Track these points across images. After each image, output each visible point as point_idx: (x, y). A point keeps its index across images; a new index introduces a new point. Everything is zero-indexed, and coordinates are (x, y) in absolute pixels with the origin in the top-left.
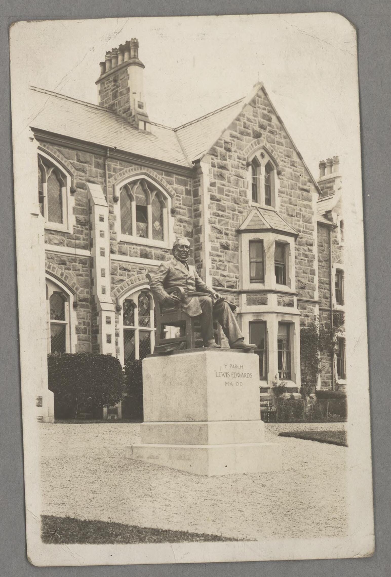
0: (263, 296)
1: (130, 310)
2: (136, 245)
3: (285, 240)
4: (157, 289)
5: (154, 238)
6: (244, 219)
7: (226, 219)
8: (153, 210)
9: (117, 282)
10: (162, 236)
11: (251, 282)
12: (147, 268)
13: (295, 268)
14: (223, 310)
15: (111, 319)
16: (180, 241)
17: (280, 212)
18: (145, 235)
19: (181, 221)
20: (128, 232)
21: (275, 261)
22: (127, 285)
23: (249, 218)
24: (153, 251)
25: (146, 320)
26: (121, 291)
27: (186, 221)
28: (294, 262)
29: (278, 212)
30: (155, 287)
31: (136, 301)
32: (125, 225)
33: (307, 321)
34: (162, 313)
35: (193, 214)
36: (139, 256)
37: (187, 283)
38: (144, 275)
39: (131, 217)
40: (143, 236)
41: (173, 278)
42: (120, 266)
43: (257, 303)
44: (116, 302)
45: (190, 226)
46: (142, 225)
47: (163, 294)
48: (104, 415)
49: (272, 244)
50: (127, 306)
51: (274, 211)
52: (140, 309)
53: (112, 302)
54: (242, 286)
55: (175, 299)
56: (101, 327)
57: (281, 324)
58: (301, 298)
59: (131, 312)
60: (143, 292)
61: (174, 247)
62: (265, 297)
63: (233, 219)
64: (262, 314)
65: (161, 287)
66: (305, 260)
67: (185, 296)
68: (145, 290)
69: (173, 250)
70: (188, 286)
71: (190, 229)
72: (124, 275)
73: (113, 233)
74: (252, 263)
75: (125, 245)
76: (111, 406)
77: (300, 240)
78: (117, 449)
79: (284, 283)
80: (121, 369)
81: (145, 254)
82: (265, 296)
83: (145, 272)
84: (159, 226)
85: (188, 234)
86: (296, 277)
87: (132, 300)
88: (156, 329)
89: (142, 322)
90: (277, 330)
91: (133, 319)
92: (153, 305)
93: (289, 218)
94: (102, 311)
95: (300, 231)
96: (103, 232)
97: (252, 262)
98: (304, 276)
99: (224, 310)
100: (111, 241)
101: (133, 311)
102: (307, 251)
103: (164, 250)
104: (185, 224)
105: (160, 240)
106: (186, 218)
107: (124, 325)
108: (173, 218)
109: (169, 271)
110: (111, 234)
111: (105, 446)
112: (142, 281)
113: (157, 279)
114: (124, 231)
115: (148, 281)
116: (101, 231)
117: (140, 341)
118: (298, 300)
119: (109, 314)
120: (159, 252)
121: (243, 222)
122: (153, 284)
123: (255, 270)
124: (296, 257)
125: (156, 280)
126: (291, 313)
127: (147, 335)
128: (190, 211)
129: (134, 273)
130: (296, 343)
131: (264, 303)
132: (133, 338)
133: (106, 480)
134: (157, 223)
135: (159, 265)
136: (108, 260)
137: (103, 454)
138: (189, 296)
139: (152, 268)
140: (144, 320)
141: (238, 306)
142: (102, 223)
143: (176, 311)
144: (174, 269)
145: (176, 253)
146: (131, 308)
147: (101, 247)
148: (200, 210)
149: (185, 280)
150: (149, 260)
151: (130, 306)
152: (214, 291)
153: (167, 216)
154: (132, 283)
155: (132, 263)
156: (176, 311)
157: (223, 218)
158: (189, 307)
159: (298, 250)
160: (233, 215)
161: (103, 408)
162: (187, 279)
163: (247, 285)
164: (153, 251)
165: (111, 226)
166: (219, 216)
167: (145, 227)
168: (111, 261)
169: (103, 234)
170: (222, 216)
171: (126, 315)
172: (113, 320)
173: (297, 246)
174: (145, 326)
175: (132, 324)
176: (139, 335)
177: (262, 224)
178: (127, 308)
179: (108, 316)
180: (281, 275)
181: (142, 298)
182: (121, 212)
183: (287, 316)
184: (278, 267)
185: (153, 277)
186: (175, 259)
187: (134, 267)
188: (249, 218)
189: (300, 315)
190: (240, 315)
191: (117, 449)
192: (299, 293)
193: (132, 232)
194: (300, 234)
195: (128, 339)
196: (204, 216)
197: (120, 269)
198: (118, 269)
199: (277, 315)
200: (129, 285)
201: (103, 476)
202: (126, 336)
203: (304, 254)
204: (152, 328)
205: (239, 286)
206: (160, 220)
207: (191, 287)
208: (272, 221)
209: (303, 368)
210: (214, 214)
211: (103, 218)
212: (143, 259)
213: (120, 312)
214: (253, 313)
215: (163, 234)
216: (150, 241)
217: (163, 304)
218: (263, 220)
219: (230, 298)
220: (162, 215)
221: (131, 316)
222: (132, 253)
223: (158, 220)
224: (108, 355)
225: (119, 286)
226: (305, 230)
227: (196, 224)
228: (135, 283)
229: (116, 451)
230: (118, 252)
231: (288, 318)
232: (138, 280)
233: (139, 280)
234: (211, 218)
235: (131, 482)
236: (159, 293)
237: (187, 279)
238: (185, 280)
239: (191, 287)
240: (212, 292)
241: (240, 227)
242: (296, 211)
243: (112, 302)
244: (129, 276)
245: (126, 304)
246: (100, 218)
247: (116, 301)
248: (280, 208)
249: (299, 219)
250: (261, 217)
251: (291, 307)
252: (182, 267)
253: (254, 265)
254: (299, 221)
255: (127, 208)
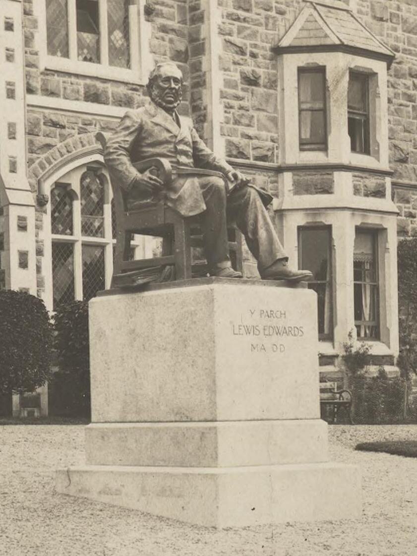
0: (325, 177)
1: (65, 204)
2: (77, 76)
3: (369, 66)
4: (118, 162)
5: (111, 63)
6: (288, 26)
7: (253, 27)
8: (109, 7)
9: (39, 149)
10: (126, 58)
11: (301, 150)
12: (99, 121)
13: (387, 122)
14: (247, 203)
15: (28, 222)
16: (162, 69)
17: (358, 12)
18: (94, 56)
19: (164, 29)
20: (61, 52)
21: (349, 107)
22: (58, 154)
23: (299, 25)
24: (110, 89)
25: (97, 224)
26: (48, 167)
27: (173, 30)
28: (386, 110)
29: (355, 12)
30: (114, 160)
31: (76, 186)
32: (54, 37)
33: (411, 226)
34: (126, 210)
35: (188, 16)
36: (82, 98)
37: (177, 152)
38: (92, 136)
39: (67, 21)
40: (90, 60)
41: (148, 141)
42: (45, 117)
43: (313, 190)
44: (36, 188)
45: (183, 40)
46: (88, 37)
47: (129, 172)
48: (14, 409)
49: (343, 75)
50: (59, 195)
51: (347, 11)
52: (84, 202)
53: (29, 188)
54: (284, 157)
55: (152, 182)
56: (9, 236)
57: (360, 231)
58: (400, 181)
59: (67, 207)
60: (89, 169)
61: (150, 80)
62: (329, 179)
63: (267, 25)
64: (323, 211)
65: (125, 159)
66: (408, 106)
67: (173, 177)
68: (94, 166)
69: (150, 86)
70: (178, 157)
71: (181, 46)
72: (52, 135)
73: (31, 54)
74: (303, 113)
75: (56, 77)
76: (28, 391)
77: (398, 66)
78: (39, 476)
79: (366, 151)
80: (48, 319)
81: (95, 94)
82: (329, 177)
83: (94, 130)
84: (121, 38)
85: (178, 56)
86: (390, 138)
87: (69, 185)
88: (115, 241)
89: (89, 228)
90: (353, 244)
91: (71, 220)
92: (110, 194)
93: (376, 25)
94: (10, 206)
95: (397, 50)
96: (13, 51)
97: (303, 110)
98: (405, 137)
99: (248, 204)
100: (28, 69)
101: (71, 205)
102: (411, 88)
103: (130, 86)
104: (171, 36)
105: (123, 66)
106: (174, 24)
107: (53, 232)
108: (149, 24)
109: (141, 128)
110: (28, 55)
111: (16, 470)
112: (88, 146)
113: (117, 142)
114: (52, 49)
115: (100, 147)
116: (7, 50)
117: (85, 264)
118: (393, 184)
119: (23, 212)
120: (122, 90)
121: (286, 32)
122: (110, 153)
123: (309, 126)
124: (390, 101)
125: (116, 145)
126: (380, 209)
127: (97, 253)
128: (181, 9)
129: (73, 131)
130: (389, 268)
131: (326, 189)
132: (70, 259)
133: (18, 536)
134: (118, 34)
135: (122, 115)
136: (22, 105)
137: (12, 486)
138: (180, 176)
139: (108, 122)
140: (91, 224)
141: (277, 196)
142: (9, 33)
143: (155, 205)
144: (150, 124)
145: (155, 92)
146: (67, 200)
147: (9, 80)
148: (202, 8)
149: (172, 146)
150: (102, 106)
151: (64, 196)
152: (228, 167)
153: (136, 21)
154: (68, 152)
155: (69, 111)
156: (155, 205)
157: (246, 25)
158: (180, 197)
159: (393, 86)
160: (267, 18)
161: (11, 394)
162: (176, 144)
163: (294, 156)
164: (110, 89)
165: (28, 40)
166: (238, 19)
167: (94, 41)
168: (27, 108)
169: (12, 56)
170: (245, 20)
171: (56, 214)
172: (31, 224)
173: (392, 79)
174: (94, 236)
175: (68, 231)
176: (83, 253)
177: (323, 35)
178: (58, 199)
179: (22, 215)
180: (361, 134)
181: (88, 180)
182: (47, 13)
183: (372, 215)
184: (354, 119)
185: (110, 139)
186: (153, 104)
187: (73, 120)
188: (299, 25)
189: (398, 214)
190: (280, 213)
191: (39, 476)
192: (396, 171)
193: (68, 51)
194: (398, 55)
195: (60, 259)
196: (209, 19)
197: (45, 124)
198: (42, 123)
199: (353, 214)
200: (62, 155)
201: (12, 527)
202: (57, 255)
203: (405, 94)
204: (109, 239)
205: (277, 157)
206: (123, 27)
207: (183, 159)
208: (343, 30)
209: (403, 317)
210: (229, 16)
211: (12, 25)
212: (89, 104)
213: (44, 208)
214: (306, 209)
215: (129, 55)
216: (104, 69)
217: (129, 193)
218: (325, 28)
219: (260, 179)
220: (126, 17)
221: (67, 216)
222: (68, 91)
223: (119, 29)
224: (21, 292)
225: (43, 156)
226: (406, 47)
227: (194, 36)
228: (74, 152)
229: (37, 479)
230: (42, 90)
231: (373, 220)
232: (80, 145)
233: (83, 146)
234: (224, 23)
235: (67, 540)
236: (121, 171)
237: (176, 144)
238: (172, 146)
239: (183, 159)
240: (224, 169)
241: (280, 40)
242: (389, 10)
243: (29, 188)
244: (63, 137)
245: (56, 192)
246: (7, 23)
247: (36, 186)
248: (358, 4)
249: (395, 25)
250: (321, 22)
251: (380, 197)
252: (166, 120)
253: (308, 116)
254: (395, 30)
255: (60, 4)
